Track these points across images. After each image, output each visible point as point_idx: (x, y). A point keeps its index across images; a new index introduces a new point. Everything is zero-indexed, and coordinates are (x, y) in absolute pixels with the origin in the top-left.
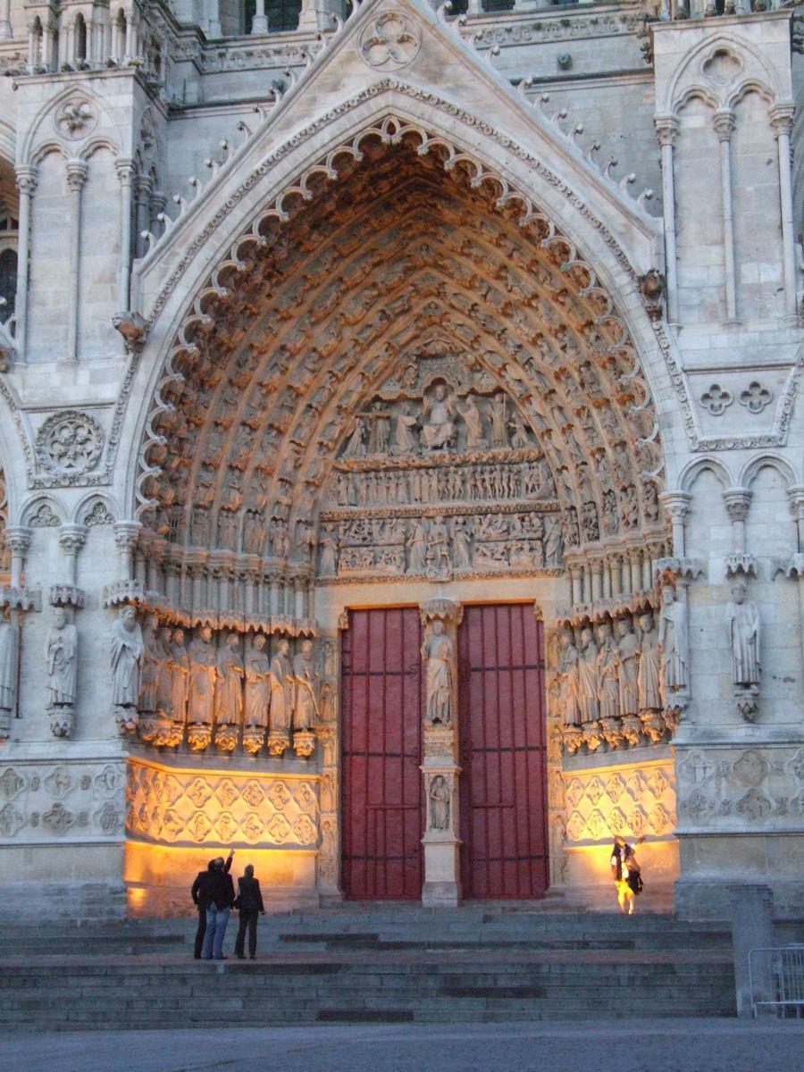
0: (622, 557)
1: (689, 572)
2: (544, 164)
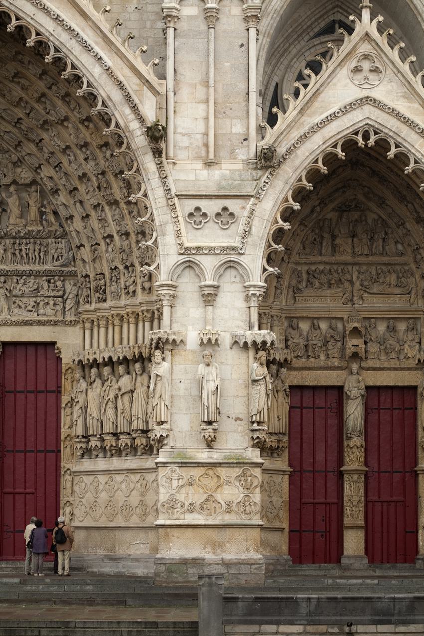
0: (123, 316)
1: (174, 340)
2: (82, 34)
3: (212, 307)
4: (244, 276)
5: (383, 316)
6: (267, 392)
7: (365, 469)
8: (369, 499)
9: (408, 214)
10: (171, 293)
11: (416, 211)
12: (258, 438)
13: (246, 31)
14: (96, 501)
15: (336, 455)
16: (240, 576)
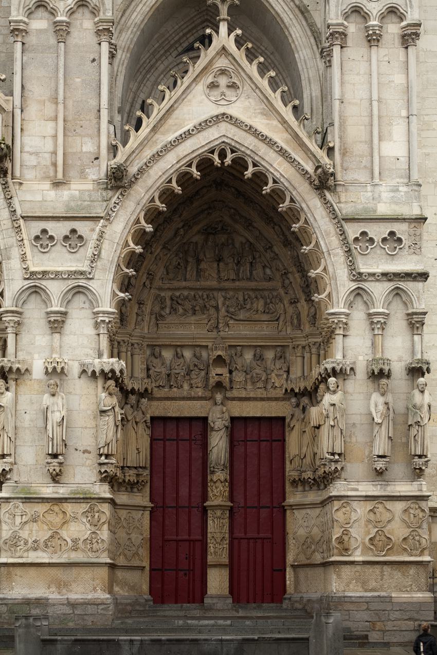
1: (18, 369)
3: (59, 334)
4: (93, 302)
5: (249, 344)
6: (115, 423)
7: (230, 504)
8: (236, 535)
9: (276, 237)
10: (16, 319)
11: (283, 233)
12: (106, 471)
13: (98, 45)
15: (201, 489)
16: (86, 617)
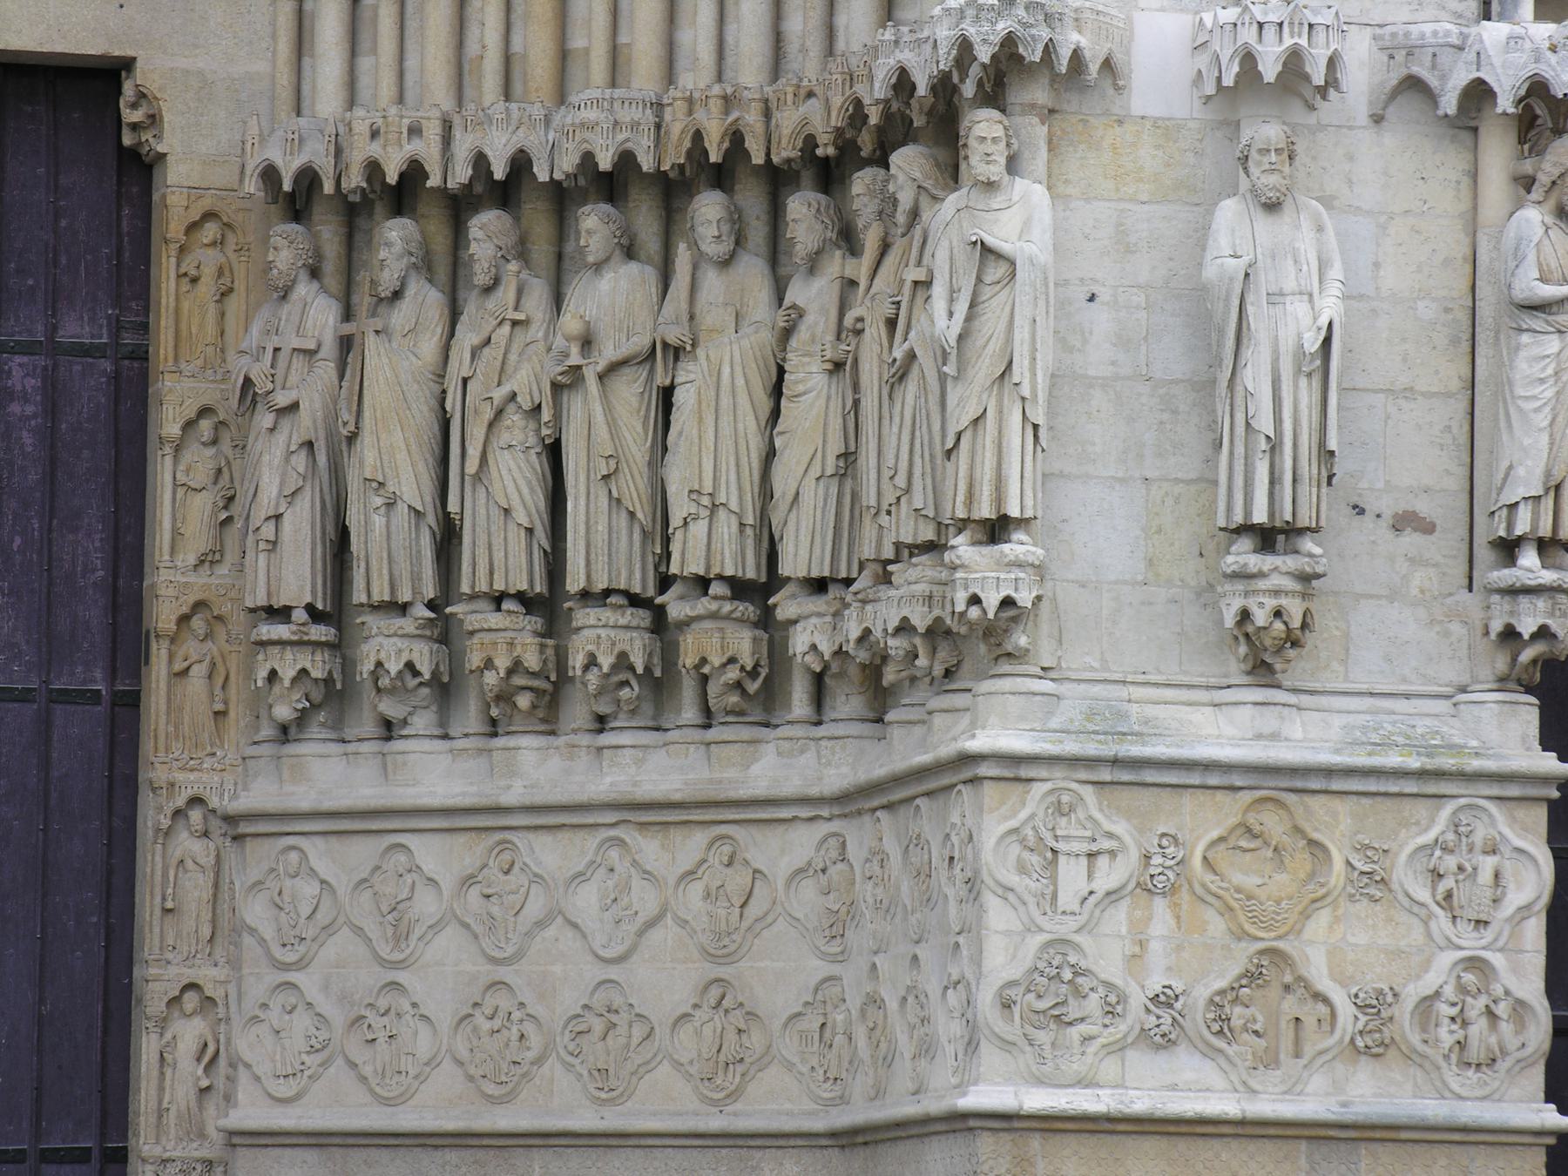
1: (1077, 56)
14: (394, 985)
